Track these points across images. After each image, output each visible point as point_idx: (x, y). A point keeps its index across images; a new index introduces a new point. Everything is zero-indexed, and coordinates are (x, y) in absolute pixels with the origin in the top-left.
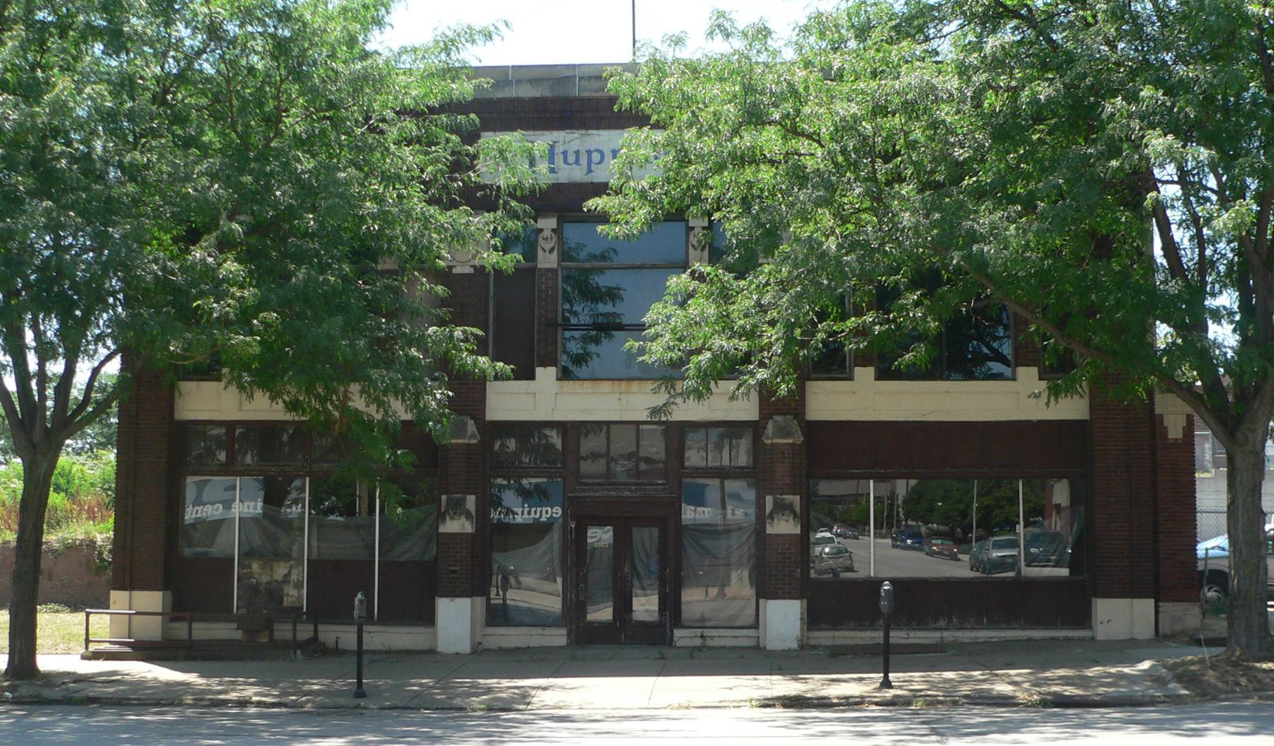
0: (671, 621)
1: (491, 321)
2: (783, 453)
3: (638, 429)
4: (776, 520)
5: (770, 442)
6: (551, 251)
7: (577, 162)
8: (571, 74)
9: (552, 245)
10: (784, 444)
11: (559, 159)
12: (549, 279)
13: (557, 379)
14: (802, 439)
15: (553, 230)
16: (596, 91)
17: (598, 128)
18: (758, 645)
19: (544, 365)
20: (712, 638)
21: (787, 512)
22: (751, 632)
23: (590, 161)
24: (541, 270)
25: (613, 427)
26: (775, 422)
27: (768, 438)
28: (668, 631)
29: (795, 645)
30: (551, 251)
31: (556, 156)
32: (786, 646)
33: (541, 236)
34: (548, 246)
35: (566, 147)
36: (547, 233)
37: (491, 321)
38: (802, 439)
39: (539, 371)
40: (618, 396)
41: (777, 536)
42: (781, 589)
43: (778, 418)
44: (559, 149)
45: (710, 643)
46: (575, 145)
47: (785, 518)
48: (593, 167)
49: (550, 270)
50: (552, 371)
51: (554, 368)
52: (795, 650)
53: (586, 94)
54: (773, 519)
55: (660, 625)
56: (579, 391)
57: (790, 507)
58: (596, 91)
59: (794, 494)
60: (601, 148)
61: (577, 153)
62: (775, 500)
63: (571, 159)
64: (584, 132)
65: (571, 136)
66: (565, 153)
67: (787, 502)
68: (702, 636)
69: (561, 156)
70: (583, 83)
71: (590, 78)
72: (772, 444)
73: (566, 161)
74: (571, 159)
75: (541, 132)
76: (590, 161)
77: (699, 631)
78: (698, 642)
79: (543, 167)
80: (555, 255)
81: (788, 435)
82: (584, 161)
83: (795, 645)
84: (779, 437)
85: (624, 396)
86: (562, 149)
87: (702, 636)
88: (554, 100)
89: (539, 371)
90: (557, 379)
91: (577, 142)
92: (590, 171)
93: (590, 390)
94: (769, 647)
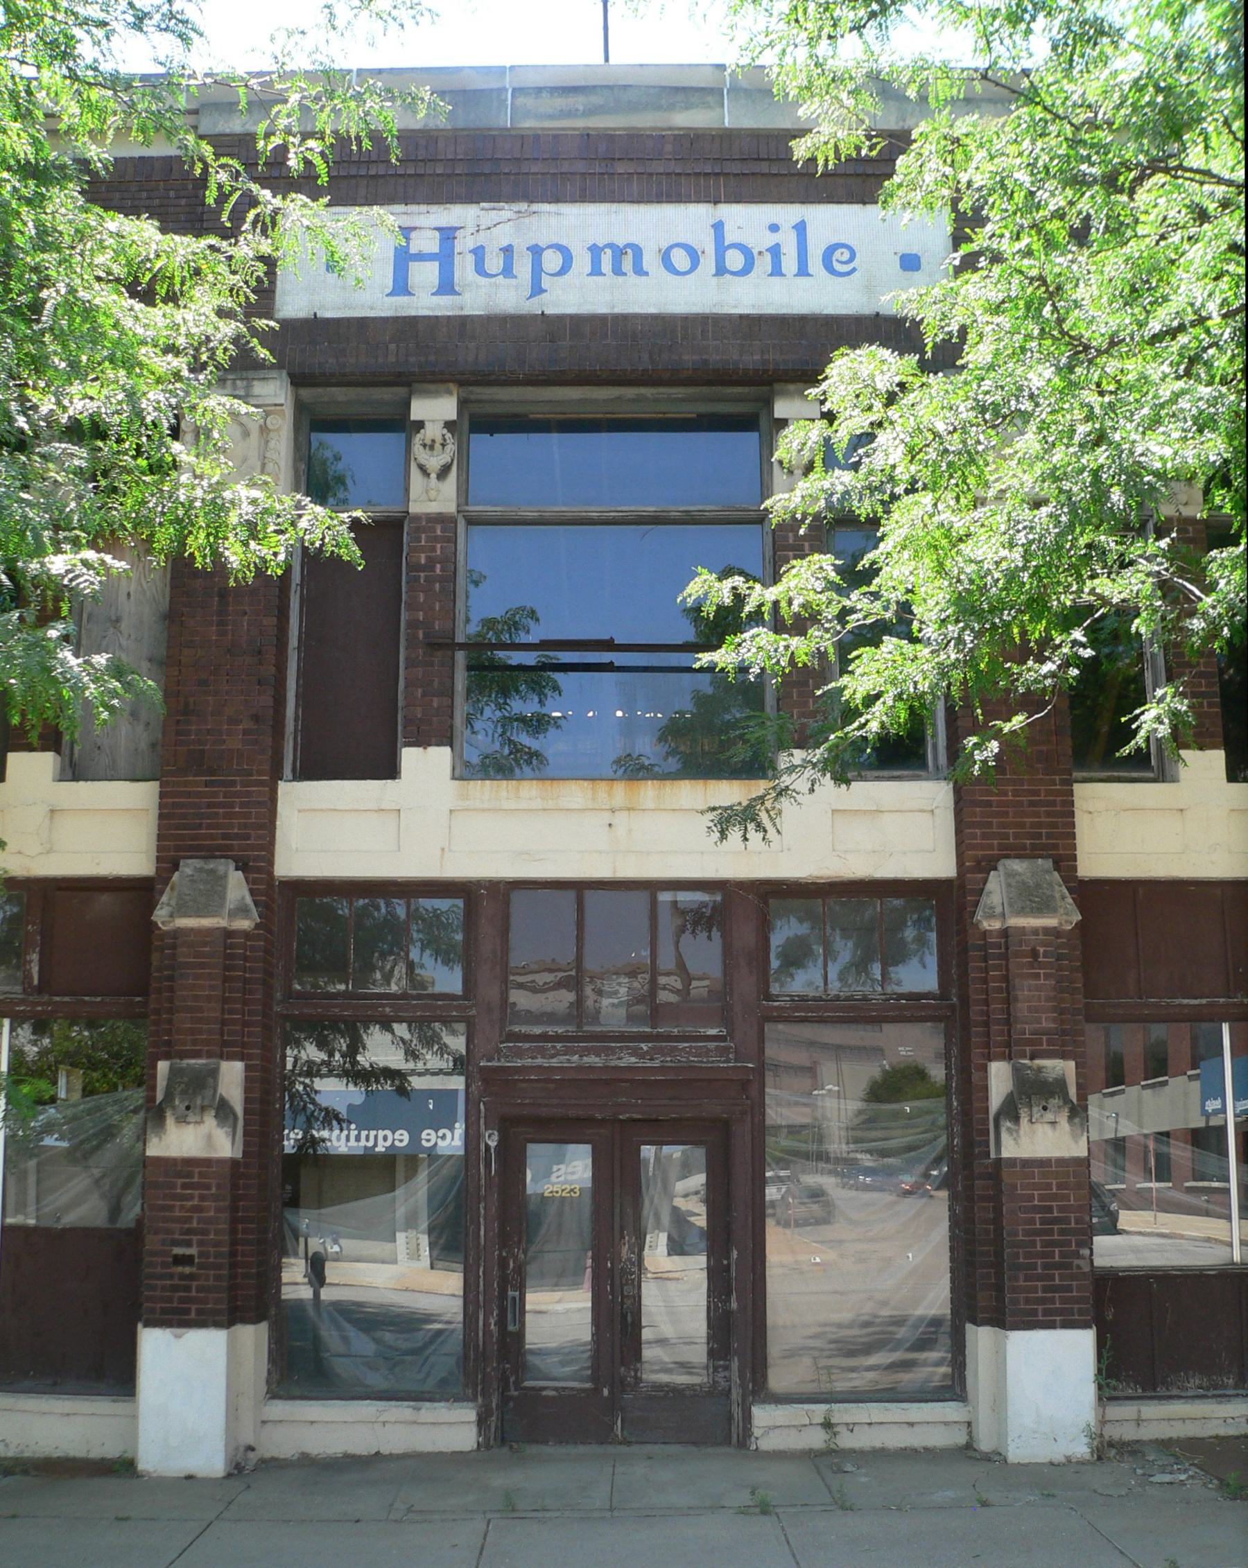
0: (743, 1386)
1: (293, 642)
2: (1034, 954)
3: (654, 903)
4: (1024, 1121)
5: (996, 925)
6: (444, 472)
7: (508, 271)
8: (494, 85)
9: (445, 458)
10: (1035, 931)
11: (464, 269)
12: (436, 539)
13: (454, 778)
14: (1077, 917)
15: (449, 425)
16: (551, 117)
17: (557, 200)
18: (969, 1446)
19: (422, 740)
20: (851, 1427)
21: (1055, 1102)
22: (950, 1411)
23: (537, 270)
24: (417, 518)
25: (589, 895)
26: (1010, 874)
27: (991, 916)
28: (737, 1412)
29: (1081, 1449)
30: (444, 472)
31: (457, 259)
32: (1057, 1452)
33: (417, 439)
34: (434, 462)
35: (481, 239)
36: (433, 431)
37: (293, 642)
38: (1077, 917)
39: (410, 757)
40: (606, 817)
41: (1027, 1163)
42: (1043, 1301)
43: (1017, 866)
44: (465, 243)
45: (846, 1441)
46: (504, 235)
47: (1049, 1116)
48: (546, 282)
49: (441, 519)
50: (441, 756)
51: (446, 751)
52: (1082, 1463)
53: (528, 124)
54: (1016, 1119)
55: (717, 1393)
56: (505, 805)
57: (1056, 1088)
58: (551, 117)
59: (1064, 1056)
60: (564, 243)
61: (508, 251)
62: (1017, 1072)
63: (494, 263)
64: (523, 206)
65: (494, 216)
66: (479, 252)
67: (1051, 1076)
68: (827, 1425)
69: (470, 259)
70: (521, 100)
71: (539, 90)
72: (1005, 933)
73: (480, 269)
74: (494, 263)
75: (423, 208)
76: (537, 270)
77: (820, 1410)
78: (816, 1439)
79: (425, 275)
80: (450, 486)
81: (1045, 906)
82: (523, 268)
83: (1081, 1449)
84: (1021, 912)
85: (621, 819)
86: (470, 243)
87: (827, 1425)
88: (455, 136)
89: (410, 757)
90: (454, 778)
91: (507, 228)
92: (537, 289)
93: (538, 804)
94: (1016, 1453)
